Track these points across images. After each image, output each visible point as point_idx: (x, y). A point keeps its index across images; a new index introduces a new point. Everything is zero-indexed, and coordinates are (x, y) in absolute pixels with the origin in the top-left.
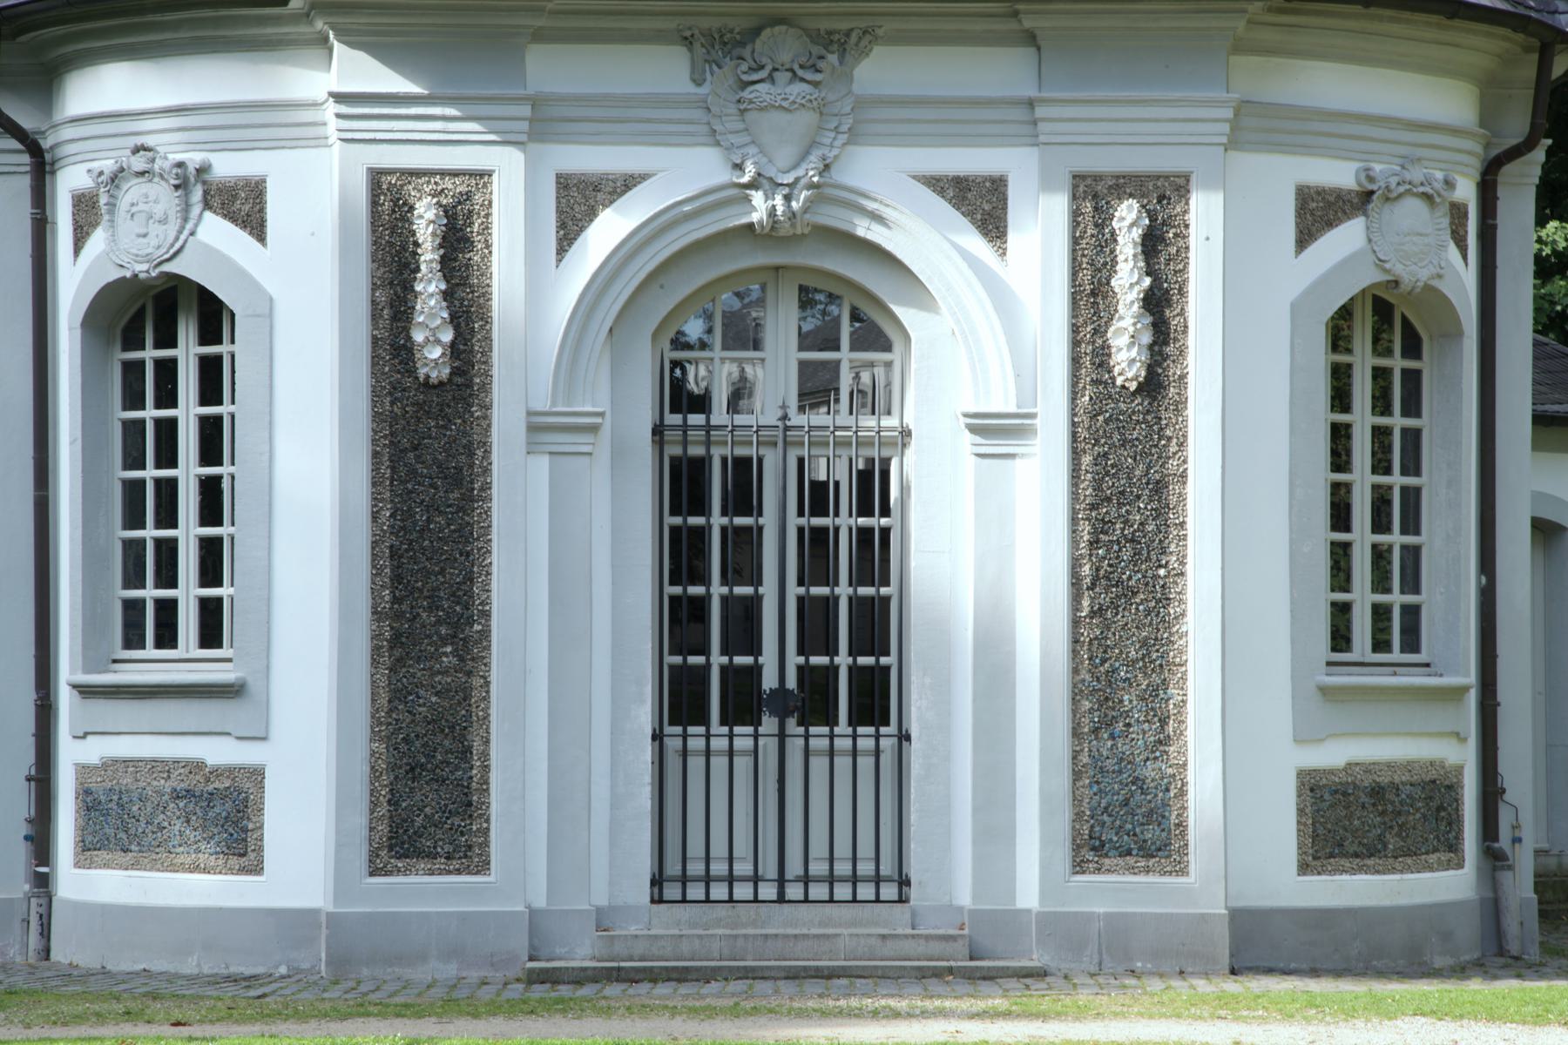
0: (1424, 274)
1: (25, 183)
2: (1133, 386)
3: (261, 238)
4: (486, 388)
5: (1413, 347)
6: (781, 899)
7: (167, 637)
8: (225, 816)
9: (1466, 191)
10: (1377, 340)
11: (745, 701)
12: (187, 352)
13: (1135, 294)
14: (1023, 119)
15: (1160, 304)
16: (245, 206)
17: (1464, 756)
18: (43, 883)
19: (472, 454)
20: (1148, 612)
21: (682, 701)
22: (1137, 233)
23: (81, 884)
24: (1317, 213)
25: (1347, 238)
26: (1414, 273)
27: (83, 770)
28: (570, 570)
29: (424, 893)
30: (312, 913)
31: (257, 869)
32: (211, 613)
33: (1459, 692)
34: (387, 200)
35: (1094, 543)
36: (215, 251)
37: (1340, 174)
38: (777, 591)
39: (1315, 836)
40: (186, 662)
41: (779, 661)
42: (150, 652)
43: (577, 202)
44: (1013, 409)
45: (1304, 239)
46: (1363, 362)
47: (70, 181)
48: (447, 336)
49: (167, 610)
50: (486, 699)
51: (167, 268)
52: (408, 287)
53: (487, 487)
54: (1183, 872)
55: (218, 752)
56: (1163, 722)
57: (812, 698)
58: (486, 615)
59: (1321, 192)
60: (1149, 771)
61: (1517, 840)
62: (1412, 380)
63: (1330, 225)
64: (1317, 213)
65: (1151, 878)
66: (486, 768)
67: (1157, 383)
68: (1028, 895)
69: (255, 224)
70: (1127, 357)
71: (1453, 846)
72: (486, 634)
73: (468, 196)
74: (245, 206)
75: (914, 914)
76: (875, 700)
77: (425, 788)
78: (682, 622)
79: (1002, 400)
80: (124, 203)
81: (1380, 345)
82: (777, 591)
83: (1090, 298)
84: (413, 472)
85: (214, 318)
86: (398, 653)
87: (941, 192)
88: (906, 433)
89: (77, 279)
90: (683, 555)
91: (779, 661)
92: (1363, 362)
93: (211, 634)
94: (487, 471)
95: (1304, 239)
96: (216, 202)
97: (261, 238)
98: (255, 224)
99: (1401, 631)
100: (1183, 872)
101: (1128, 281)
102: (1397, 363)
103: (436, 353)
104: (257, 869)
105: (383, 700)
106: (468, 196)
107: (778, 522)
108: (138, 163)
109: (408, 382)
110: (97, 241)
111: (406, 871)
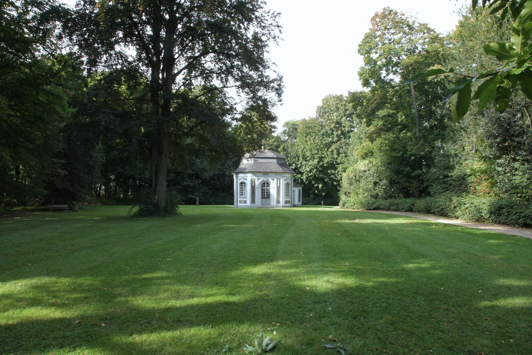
8: (245, 202)
10: (287, 184)
14: (275, 177)
16: (246, 179)
21: (262, 198)
23: (239, 204)
24: (285, 180)
28: (258, 193)
29: (253, 205)
34: (252, 180)
36: (245, 181)
38: (266, 194)
40: (243, 196)
43: (258, 179)
57: (267, 198)
64: (285, 180)
74: (246, 179)
76: (269, 198)
77: (253, 201)
78: (262, 195)
82: (266, 194)
83: (277, 183)
85: (245, 183)
89: (239, 182)
90: (262, 192)
91: (266, 196)
99: (288, 195)
107: (266, 191)
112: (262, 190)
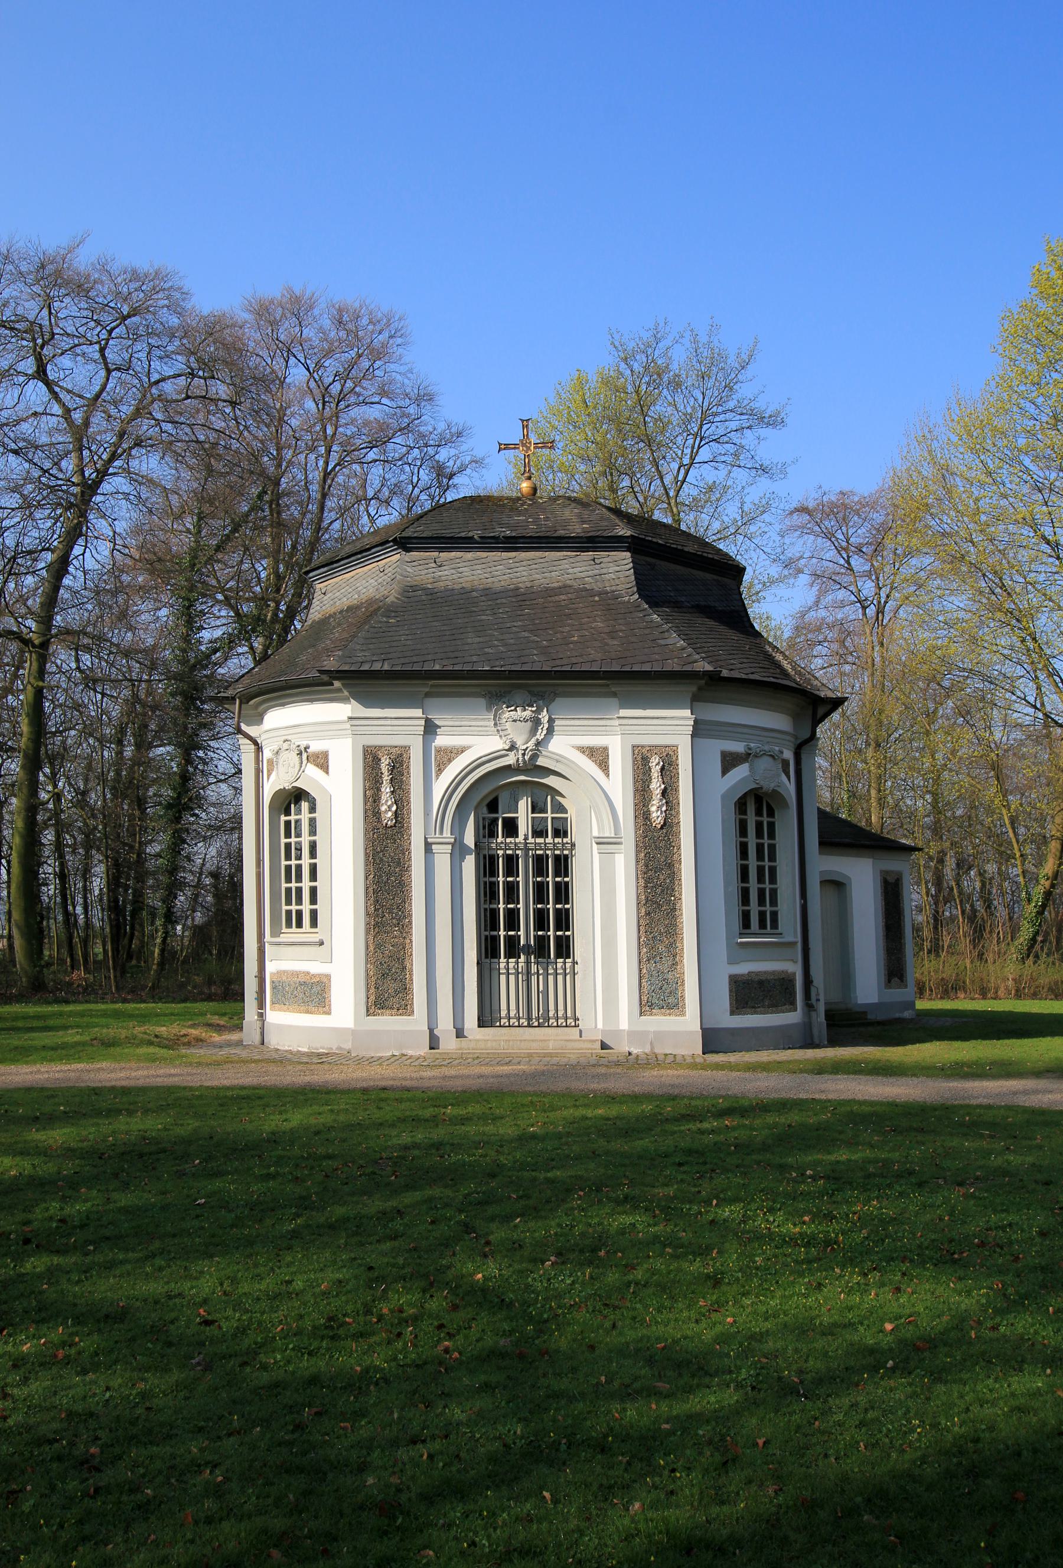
0: (772, 785)
1: (253, 755)
2: (659, 826)
3: (327, 773)
4: (409, 828)
5: (771, 813)
6: (529, 1026)
7: (299, 925)
9: (788, 755)
11: (513, 948)
12: (305, 816)
13: (659, 791)
15: (669, 793)
16: (322, 761)
17: (796, 969)
18: (261, 1016)
19: (404, 854)
20: (668, 914)
22: (658, 768)
23: (275, 1017)
24: (729, 762)
25: (741, 772)
26: (768, 785)
27: (272, 974)
29: (388, 1022)
30: (349, 1029)
31: (329, 1013)
32: (314, 914)
33: (792, 944)
34: (371, 758)
35: (646, 887)
36: (311, 778)
37: (738, 747)
38: (526, 906)
39: (737, 1000)
40: (306, 933)
41: (526, 934)
42: (294, 929)
44: (613, 835)
45: (725, 771)
46: (751, 820)
47: (267, 754)
48: (394, 808)
49: (299, 914)
50: (411, 948)
51: (295, 784)
52: (379, 790)
53: (410, 866)
54: (684, 1015)
55: (315, 968)
56: (675, 956)
58: (411, 916)
59: (731, 754)
60: (670, 976)
61: (818, 1000)
62: (771, 826)
63: (735, 766)
64: (729, 762)
65: (671, 1017)
66: (411, 975)
67: (669, 825)
68: (624, 1025)
69: (325, 767)
70: (657, 816)
71: (793, 1002)
72: (410, 923)
73: (401, 755)
74: (322, 761)
75: (581, 1031)
77: (387, 983)
79: (609, 832)
80: (281, 761)
81: (759, 813)
82: (526, 906)
84: (381, 860)
86: (377, 930)
87: (583, 752)
88: (573, 845)
89: (269, 790)
91: (526, 934)
92: (751, 820)
93: (314, 923)
94: (410, 859)
95: (725, 771)
96: (311, 759)
97: (327, 773)
98: (325, 767)
99: (769, 922)
100: (684, 1015)
101: (656, 786)
102: (765, 819)
103: (390, 814)
104: (329, 1013)
105: (372, 948)
106: (401, 755)
108: (286, 746)
109: (379, 826)
110: (273, 776)
111: (382, 1014)
112: (487, 866)
